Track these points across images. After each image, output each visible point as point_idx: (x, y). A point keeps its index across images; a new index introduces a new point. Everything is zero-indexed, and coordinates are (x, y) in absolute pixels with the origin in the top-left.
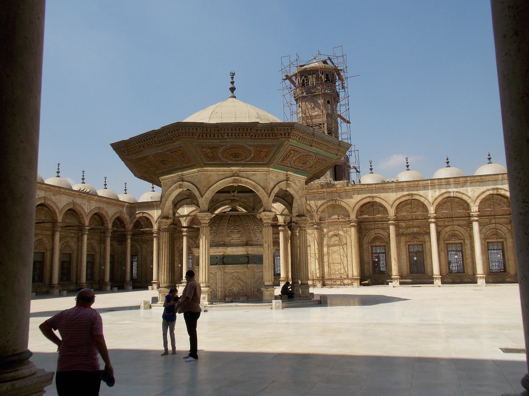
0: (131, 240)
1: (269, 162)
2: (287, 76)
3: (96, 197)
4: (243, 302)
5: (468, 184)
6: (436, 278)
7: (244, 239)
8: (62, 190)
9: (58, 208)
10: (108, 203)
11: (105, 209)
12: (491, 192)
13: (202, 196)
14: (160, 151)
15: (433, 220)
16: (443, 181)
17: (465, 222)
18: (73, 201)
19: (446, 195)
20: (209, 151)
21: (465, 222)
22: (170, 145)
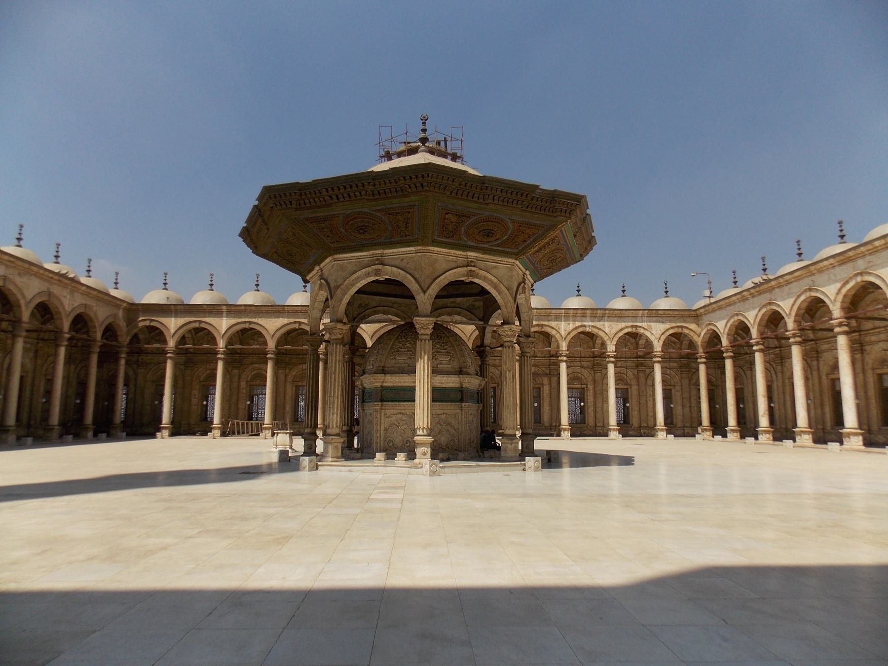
3: (84, 288)
4: (464, 460)
6: (565, 430)
7: (456, 365)
8: (34, 268)
9: (24, 297)
10: (98, 299)
11: (94, 309)
12: (630, 330)
13: (425, 292)
14: (365, 210)
15: (565, 358)
16: (579, 312)
17: (589, 364)
18: (48, 289)
19: (581, 330)
20: (454, 219)
21: (589, 364)
22: (394, 201)
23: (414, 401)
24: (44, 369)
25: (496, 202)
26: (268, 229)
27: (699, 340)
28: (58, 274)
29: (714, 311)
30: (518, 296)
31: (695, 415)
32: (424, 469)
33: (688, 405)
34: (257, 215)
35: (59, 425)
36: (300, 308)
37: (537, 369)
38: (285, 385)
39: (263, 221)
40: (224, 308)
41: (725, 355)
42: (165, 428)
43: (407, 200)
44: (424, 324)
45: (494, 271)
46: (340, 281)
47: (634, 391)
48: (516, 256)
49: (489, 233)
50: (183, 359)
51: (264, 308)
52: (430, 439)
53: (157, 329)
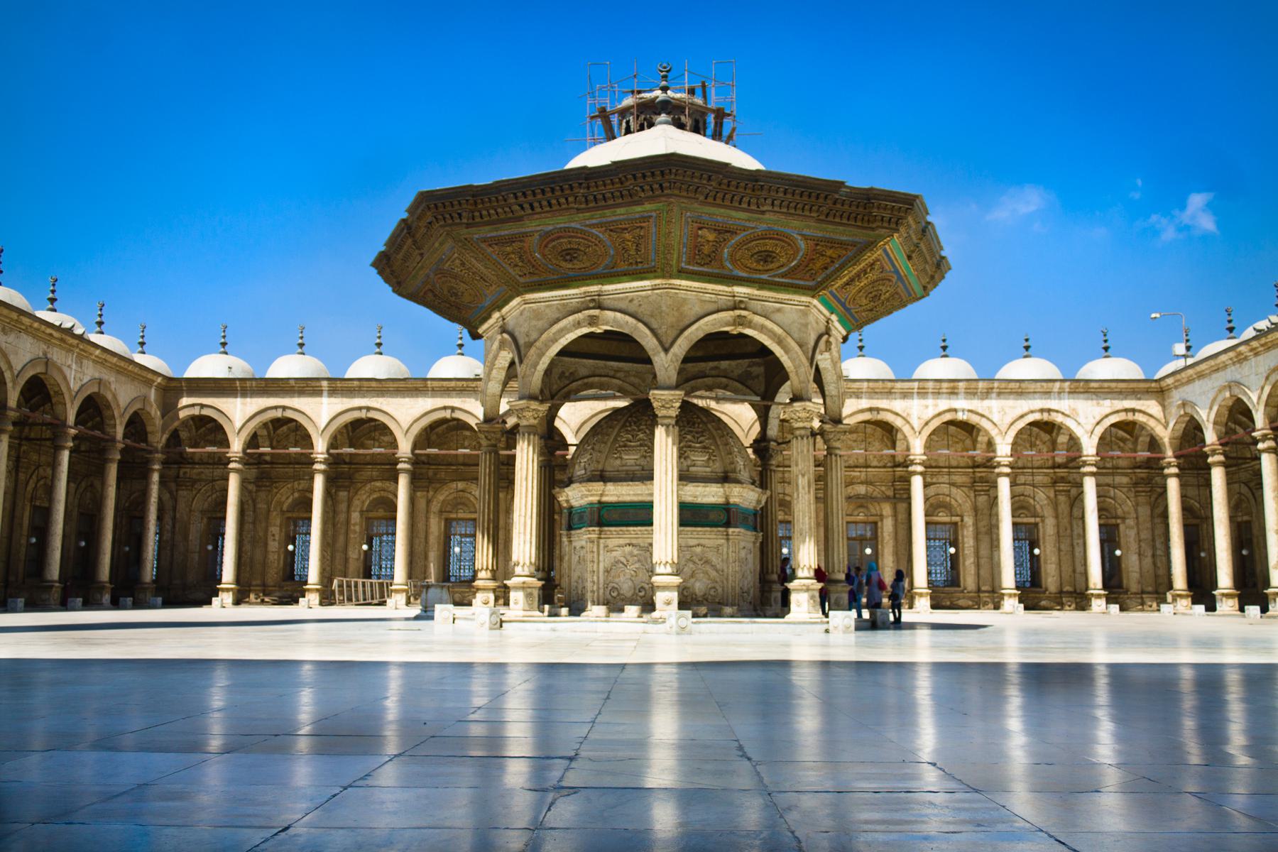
0: (161, 477)
1: (820, 283)
2: (603, 110)
3: (98, 352)
5: (994, 395)
6: (921, 595)
7: (717, 467)
8: (26, 320)
10: (120, 371)
11: (113, 387)
12: (1037, 416)
13: (666, 350)
14: (573, 225)
16: (945, 385)
18: (45, 354)
19: (948, 417)
20: (711, 237)
22: (619, 211)
23: (651, 524)
24: (30, 488)
25: (776, 209)
26: (422, 255)
27: (1165, 435)
28: (59, 328)
29: (1190, 381)
30: (818, 357)
31: (1161, 572)
32: (667, 625)
33: (1149, 553)
34: (406, 233)
35: (60, 581)
36: (453, 384)
37: (870, 489)
38: (427, 518)
39: (415, 242)
40: (325, 383)
41: (1210, 460)
42: (227, 590)
43: (639, 209)
44: (666, 401)
45: (777, 317)
46: (534, 335)
47: (1048, 528)
48: (812, 291)
49: (767, 257)
50: (253, 472)
51: (391, 384)
52: (677, 580)
53: (215, 421)
